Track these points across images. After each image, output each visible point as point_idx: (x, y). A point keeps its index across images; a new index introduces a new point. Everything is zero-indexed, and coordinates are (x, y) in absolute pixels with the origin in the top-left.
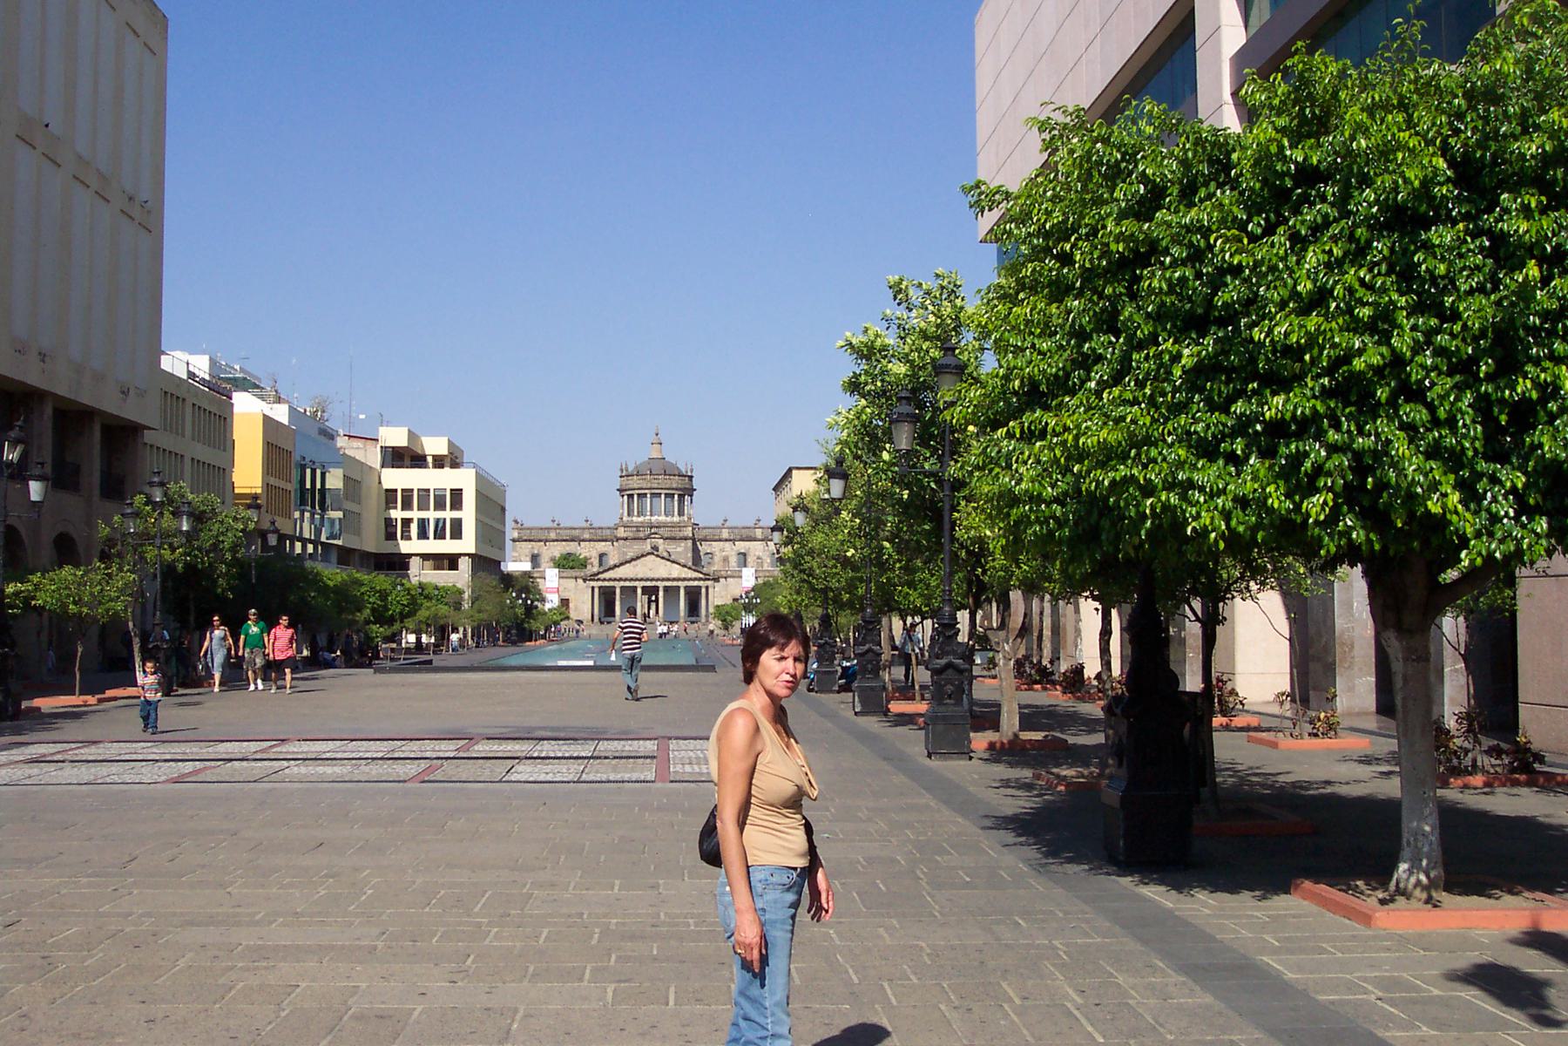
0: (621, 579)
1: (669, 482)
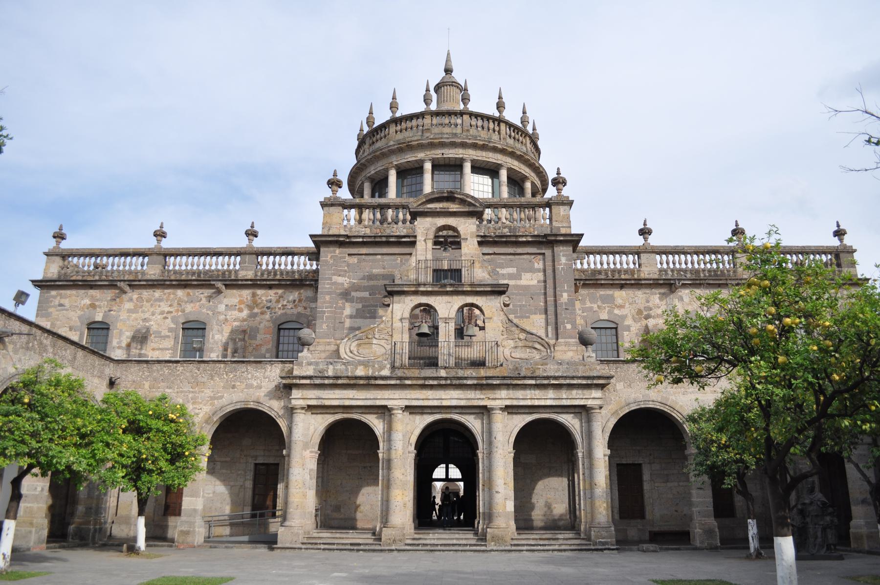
1: (484, 134)
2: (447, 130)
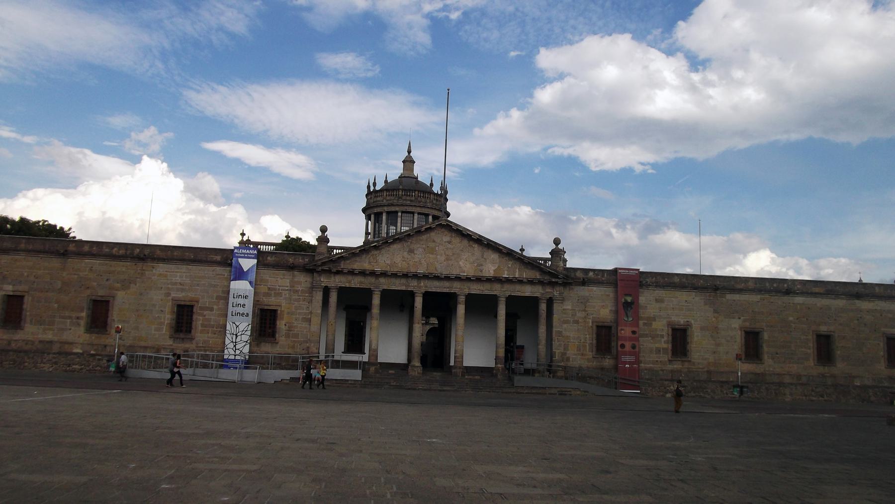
0: (384, 274)
1: (423, 200)
2: (408, 198)
